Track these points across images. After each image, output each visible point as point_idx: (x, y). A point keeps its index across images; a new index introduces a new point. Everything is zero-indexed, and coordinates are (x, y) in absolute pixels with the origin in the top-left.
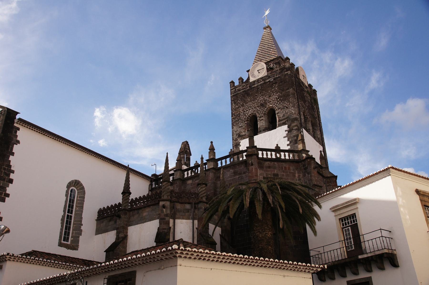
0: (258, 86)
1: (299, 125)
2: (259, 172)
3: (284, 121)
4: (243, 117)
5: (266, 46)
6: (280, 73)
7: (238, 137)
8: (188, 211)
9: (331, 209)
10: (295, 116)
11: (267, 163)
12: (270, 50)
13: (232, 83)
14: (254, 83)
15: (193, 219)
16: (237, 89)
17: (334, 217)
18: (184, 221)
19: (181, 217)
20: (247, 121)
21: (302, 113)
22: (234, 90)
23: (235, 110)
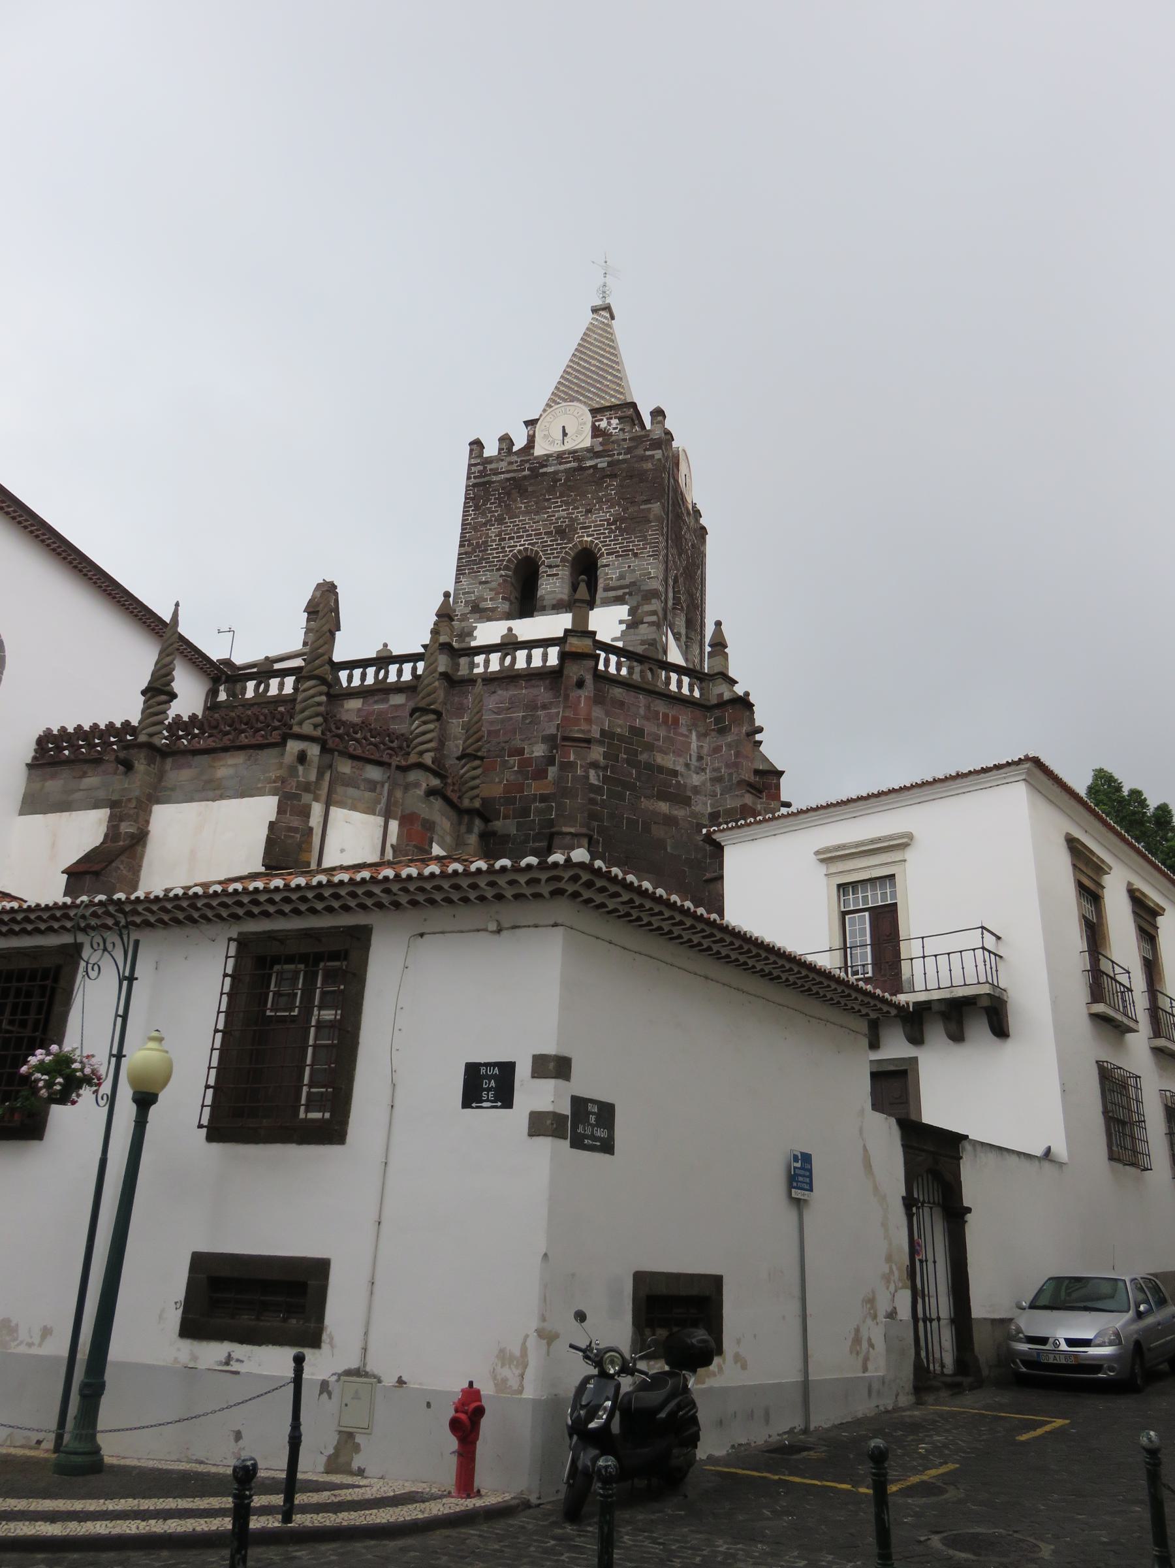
0: (556, 473)
1: (661, 614)
2: (598, 712)
3: (620, 593)
4: (492, 553)
5: (593, 362)
6: (629, 451)
7: (472, 612)
8: (373, 786)
9: (817, 853)
10: (656, 585)
11: (618, 692)
12: (606, 379)
13: (477, 445)
14: (547, 460)
15: (387, 815)
16: (489, 467)
17: (825, 879)
18: (357, 816)
19: (350, 801)
20: (507, 568)
21: (671, 582)
22: (480, 468)
23: (475, 529)
